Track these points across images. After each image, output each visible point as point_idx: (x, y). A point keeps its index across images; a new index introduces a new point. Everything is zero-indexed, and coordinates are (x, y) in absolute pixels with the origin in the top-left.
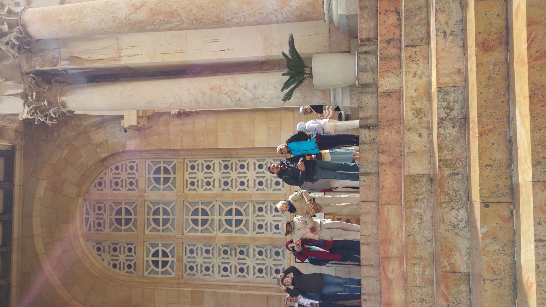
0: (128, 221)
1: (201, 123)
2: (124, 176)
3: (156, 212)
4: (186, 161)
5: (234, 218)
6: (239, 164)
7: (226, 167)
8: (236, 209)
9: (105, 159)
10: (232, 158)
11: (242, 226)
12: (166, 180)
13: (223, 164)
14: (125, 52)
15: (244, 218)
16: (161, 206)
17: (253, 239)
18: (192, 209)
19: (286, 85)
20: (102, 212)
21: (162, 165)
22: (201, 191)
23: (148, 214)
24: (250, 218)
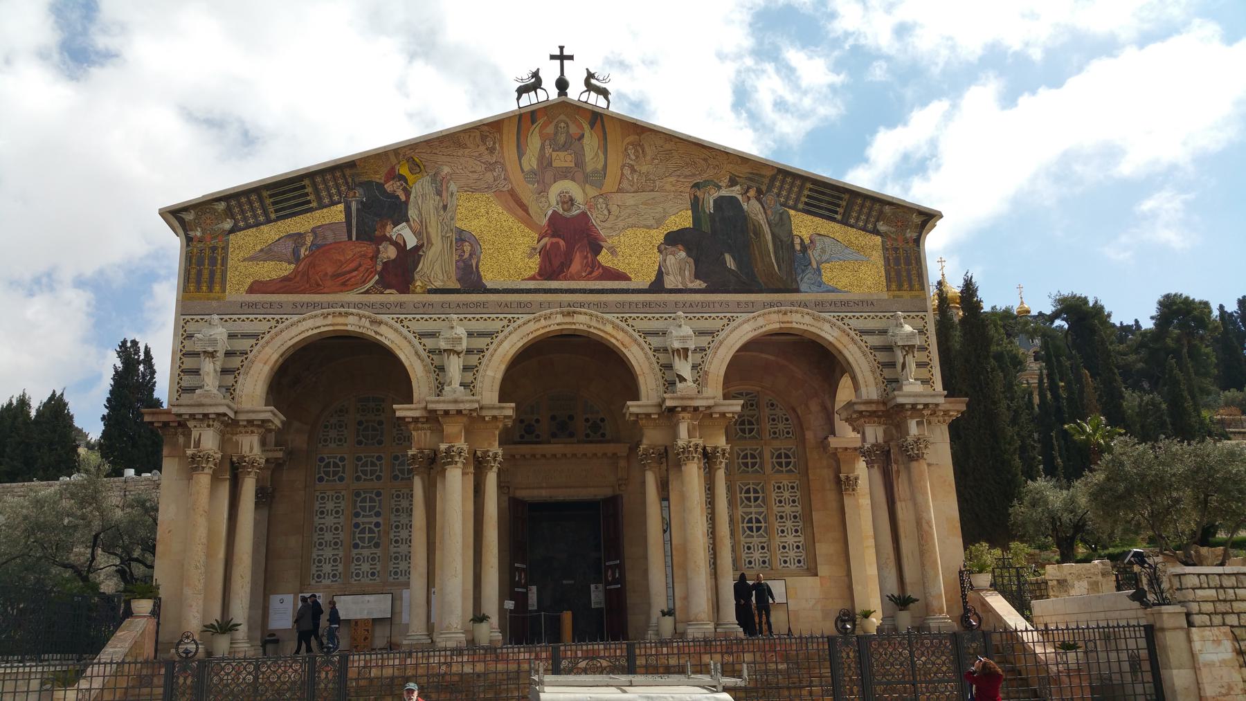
0: (743, 431)
1: (831, 496)
2: (781, 426)
3: (753, 457)
4: (797, 482)
5: (754, 525)
6: (799, 528)
7: (795, 517)
8: (761, 527)
9: (794, 410)
10: (804, 522)
11: (748, 532)
12: (780, 464)
13: (797, 515)
14: (903, 503)
15: (754, 534)
16: (758, 460)
17: (739, 542)
18: (758, 488)
19: (893, 596)
20: (749, 408)
21: (792, 460)
22: (774, 495)
23: (750, 449)
24: (755, 539)
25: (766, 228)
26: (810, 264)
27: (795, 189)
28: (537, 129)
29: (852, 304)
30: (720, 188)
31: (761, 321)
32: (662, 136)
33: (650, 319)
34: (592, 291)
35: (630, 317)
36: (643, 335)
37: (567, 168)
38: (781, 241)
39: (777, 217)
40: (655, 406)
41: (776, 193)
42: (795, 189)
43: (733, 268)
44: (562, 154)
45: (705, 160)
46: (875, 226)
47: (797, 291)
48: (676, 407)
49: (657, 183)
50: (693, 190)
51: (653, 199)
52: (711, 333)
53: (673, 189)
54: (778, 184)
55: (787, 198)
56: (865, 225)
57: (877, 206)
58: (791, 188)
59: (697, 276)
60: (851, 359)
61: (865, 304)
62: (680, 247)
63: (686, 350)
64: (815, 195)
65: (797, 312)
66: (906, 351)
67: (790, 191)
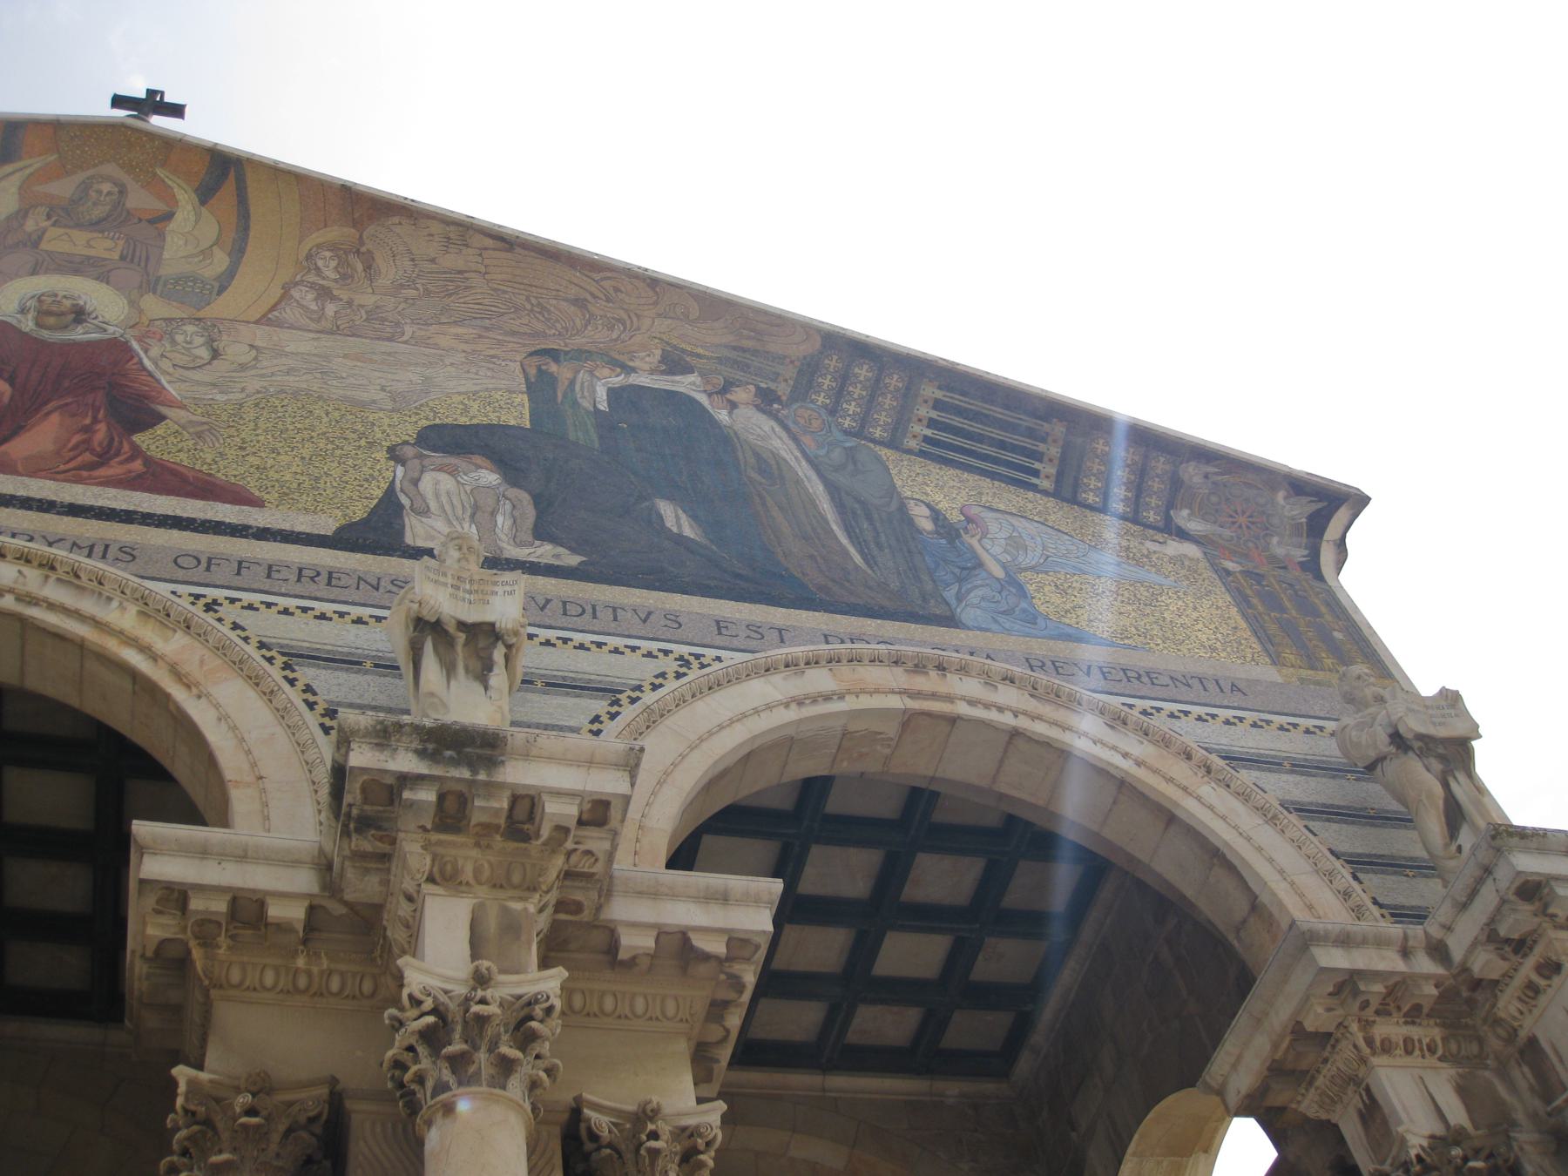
25: (803, 470)
26: (980, 565)
27: (888, 401)
28: (16, 179)
29: (1165, 680)
30: (634, 370)
31: (820, 680)
32: (436, 228)
33: (322, 617)
34: (75, 510)
35: (233, 601)
36: (280, 660)
37: (89, 258)
38: (863, 504)
39: (837, 455)
40: (288, 861)
41: (825, 406)
42: (888, 401)
43: (689, 530)
44: (81, 236)
45: (579, 303)
46: (1168, 520)
47: (950, 621)
48: (405, 780)
49: (409, 330)
50: (535, 359)
51: (389, 354)
52: (610, 692)
53: (464, 346)
54: (827, 382)
55: (864, 420)
56: (1136, 511)
57: (1160, 464)
58: (872, 398)
59: (541, 533)
60: (1222, 833)
61: (1211, 686)
62: (478, 459)
63: (483, 636)
64: (956, 421)
65: (963, 670)
66: (1442, 758)
67: (870, 403)
